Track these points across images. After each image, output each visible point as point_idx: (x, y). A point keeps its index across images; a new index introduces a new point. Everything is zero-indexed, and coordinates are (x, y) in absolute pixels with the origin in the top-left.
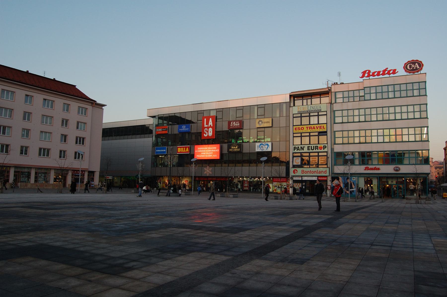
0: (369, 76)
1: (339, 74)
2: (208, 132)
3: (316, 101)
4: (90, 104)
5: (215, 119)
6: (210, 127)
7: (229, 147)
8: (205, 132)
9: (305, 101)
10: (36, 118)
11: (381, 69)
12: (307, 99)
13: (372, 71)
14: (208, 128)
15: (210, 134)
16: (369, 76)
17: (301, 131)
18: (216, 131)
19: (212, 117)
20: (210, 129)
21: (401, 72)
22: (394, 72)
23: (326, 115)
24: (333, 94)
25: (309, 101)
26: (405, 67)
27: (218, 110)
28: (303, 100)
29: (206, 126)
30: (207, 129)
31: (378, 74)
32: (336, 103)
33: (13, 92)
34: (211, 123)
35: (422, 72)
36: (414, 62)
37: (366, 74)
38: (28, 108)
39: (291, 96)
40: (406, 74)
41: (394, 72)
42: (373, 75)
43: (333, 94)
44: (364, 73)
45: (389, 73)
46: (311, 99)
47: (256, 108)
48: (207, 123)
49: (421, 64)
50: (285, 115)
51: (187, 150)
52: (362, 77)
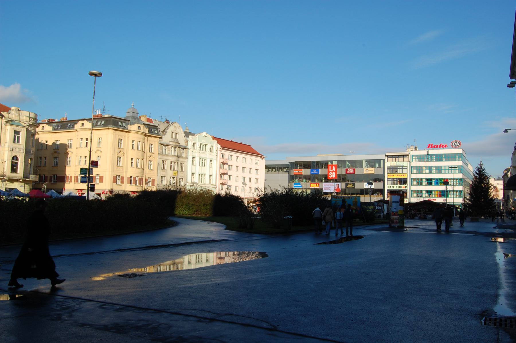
0: (432, 147)
3: (401, 159)
7: (347, 185)
9: (394, 159)
11: (439, 145)
14: (332, 172)
15: (334, 176)
16: (432, 147)
19: (335, 166)
20: (334, 173)
25: (397, 159)
31: (437, 147)
34: (334, 169)
42: (434, 147)
44: (429, 145)
45: (443, 147)
47: (364, 161)
48: (332, 169)
51: (318, 185)
52: (429, 147)
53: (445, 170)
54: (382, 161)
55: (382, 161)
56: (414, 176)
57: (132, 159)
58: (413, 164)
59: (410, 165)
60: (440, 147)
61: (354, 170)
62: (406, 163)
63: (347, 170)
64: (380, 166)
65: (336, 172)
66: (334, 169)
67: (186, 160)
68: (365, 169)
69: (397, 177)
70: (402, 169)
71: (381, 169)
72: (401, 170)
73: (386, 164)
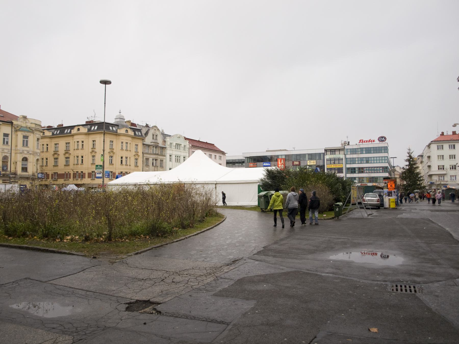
0: (362, 142)
1: (347, 137)
5: (285, 160)
11: (368, 140)
13: (364, 140)
16: (362, 142)
17: (330, 167)
19: (283, 159)
21: (377, 141)
22: (374, 141)
24: (346, 150)
26: (379, 139)
27: (286, 156)
29: (279, 163)
35: (386, 142)
36: (382, 137)
37: (361, 141)
40: (379, 142)
41: (374, 141)
42: (364, 142)
43: (346, 150)
44: (360, 141)
45: (371, 142)
47: (307, 155)
49: (385, 138)
50: (322, 159)
53: (374, 160)
56: (348, 166)
57: (122, 158)
58: (348, 156)
60: (369, 142)
61: (299, 162)
62: (342, 156)
63: (293, 162)
64: (320, 159)
67: (165, 158)
68: (308, 161)
69: (334, 167)
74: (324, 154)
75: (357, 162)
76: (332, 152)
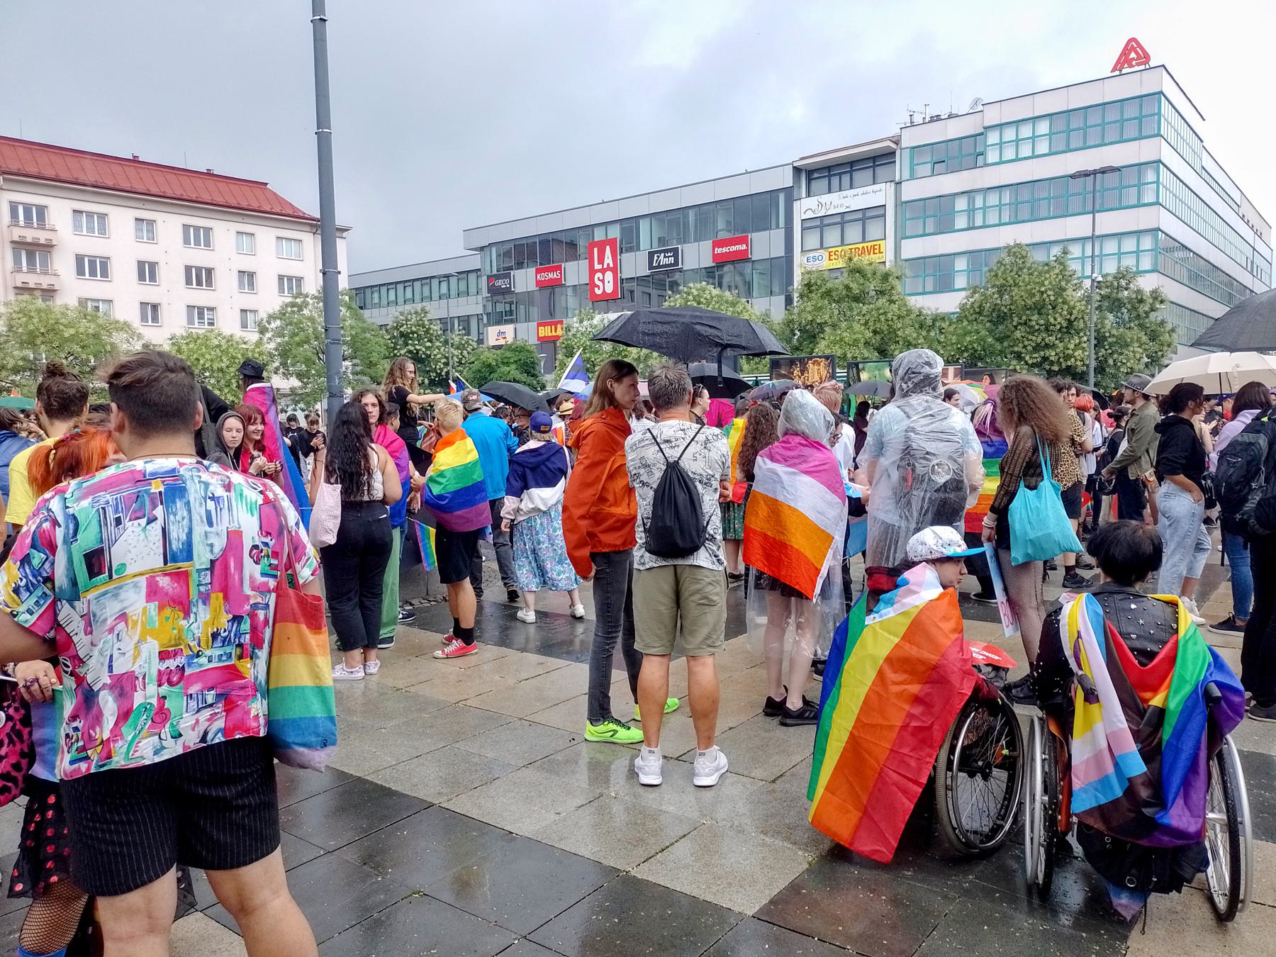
2: (603, 281)
4: (308, 229)
6: (609, 268)
8: (597, 282)
10: (172, 275)
12: (840, 174)
14: (603, 271)
18: (622, 280)
19: (612, 243)
20: (609, 276)
23: (884, 215)
24: (906, 154)
28: (829, 177)
29: (598, 267)
30: (599, 275)
32: (912, 177)
33: (102, 216)
34: (608, 260)
38: (148, 253)
39: (797, 170)
46: (851, 172)
48: (601, 261)
50: (782, 223)
54: (782, 197)
55: (782, 197)
58: (911, 191)
59: (898, 194)
61: (675, 251)
65: (614, 270)
66: (608, 260)
70: (864, 220)
71: (778, 235)
72: (859, 226)
73: (796, 205)
74: (788, 191)
75: (961, 222)
76: (835, 181)
